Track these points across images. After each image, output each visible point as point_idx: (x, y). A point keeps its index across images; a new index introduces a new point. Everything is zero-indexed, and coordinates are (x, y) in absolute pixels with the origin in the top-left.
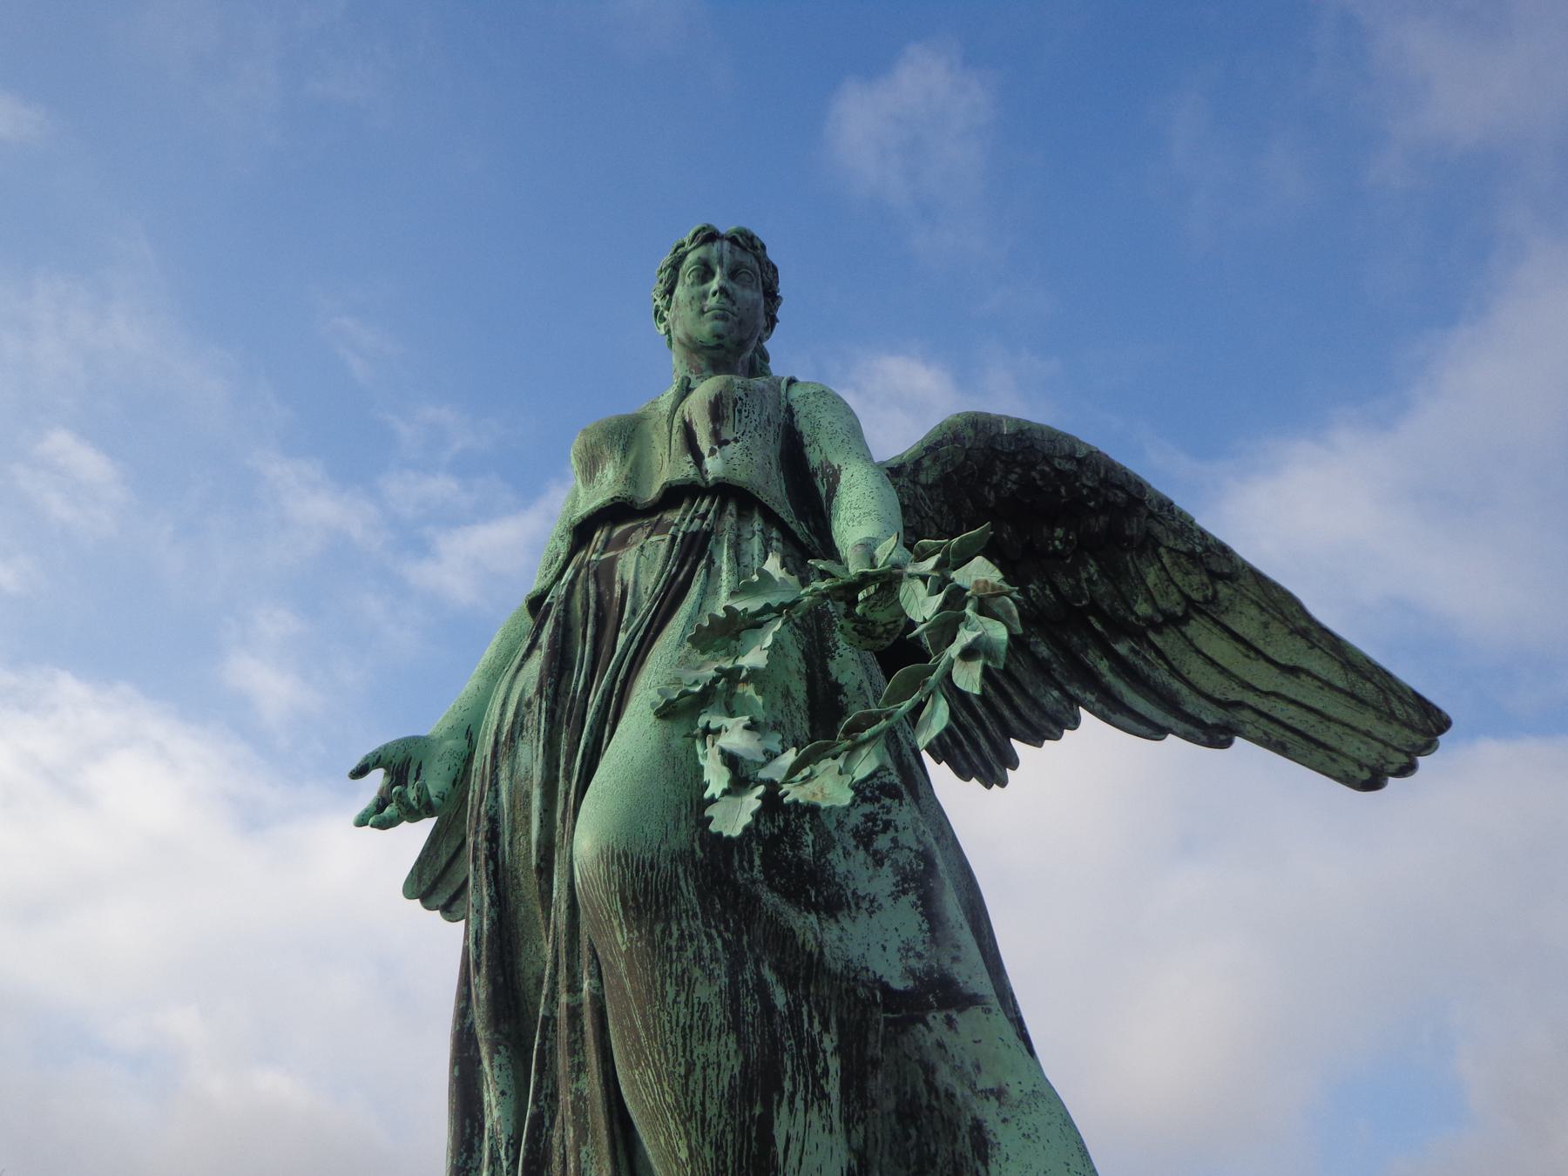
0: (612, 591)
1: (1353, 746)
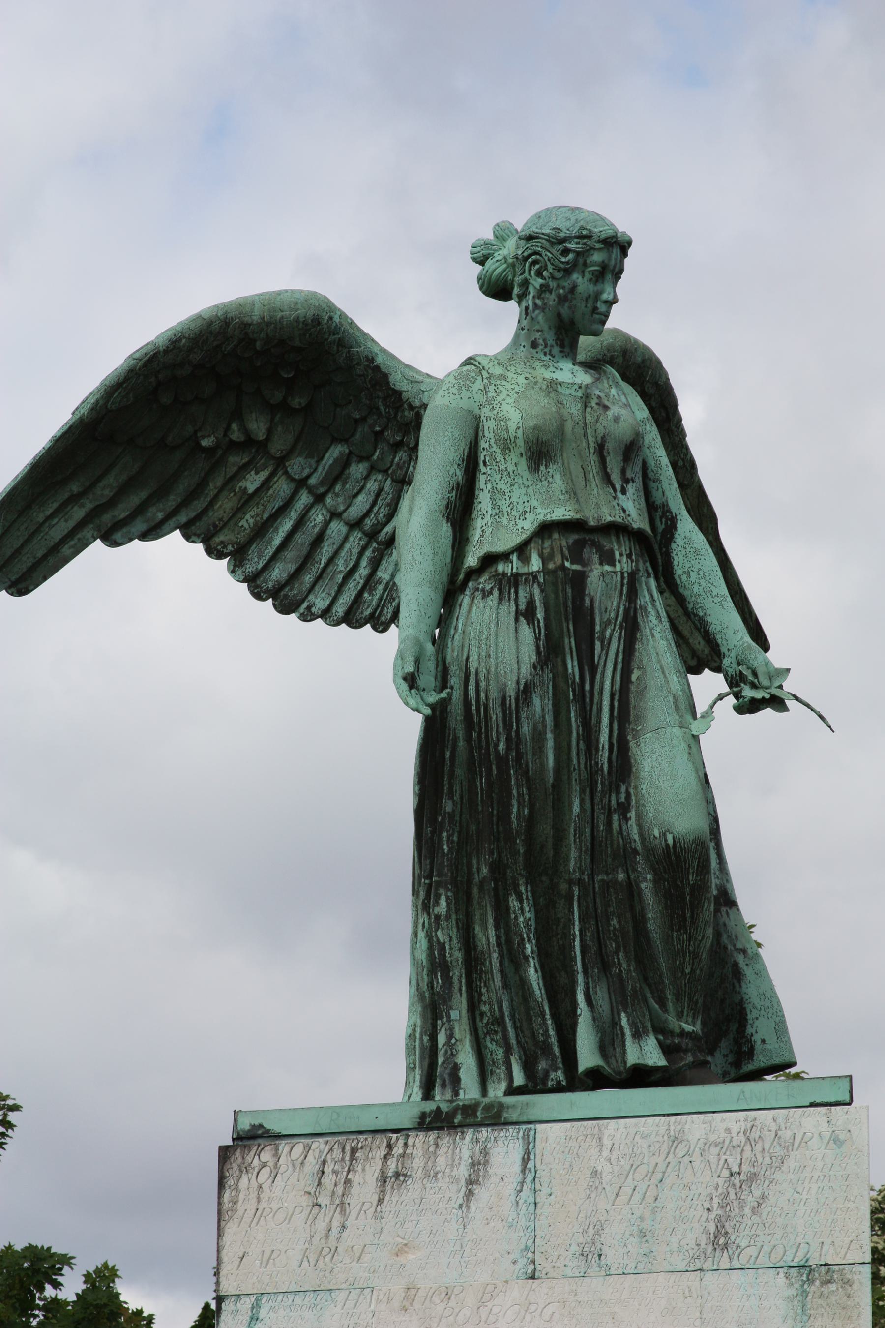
0: (583, 600)
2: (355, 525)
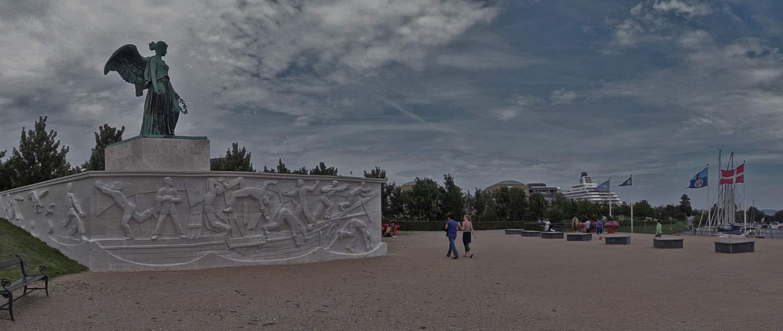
2: (134, 73)
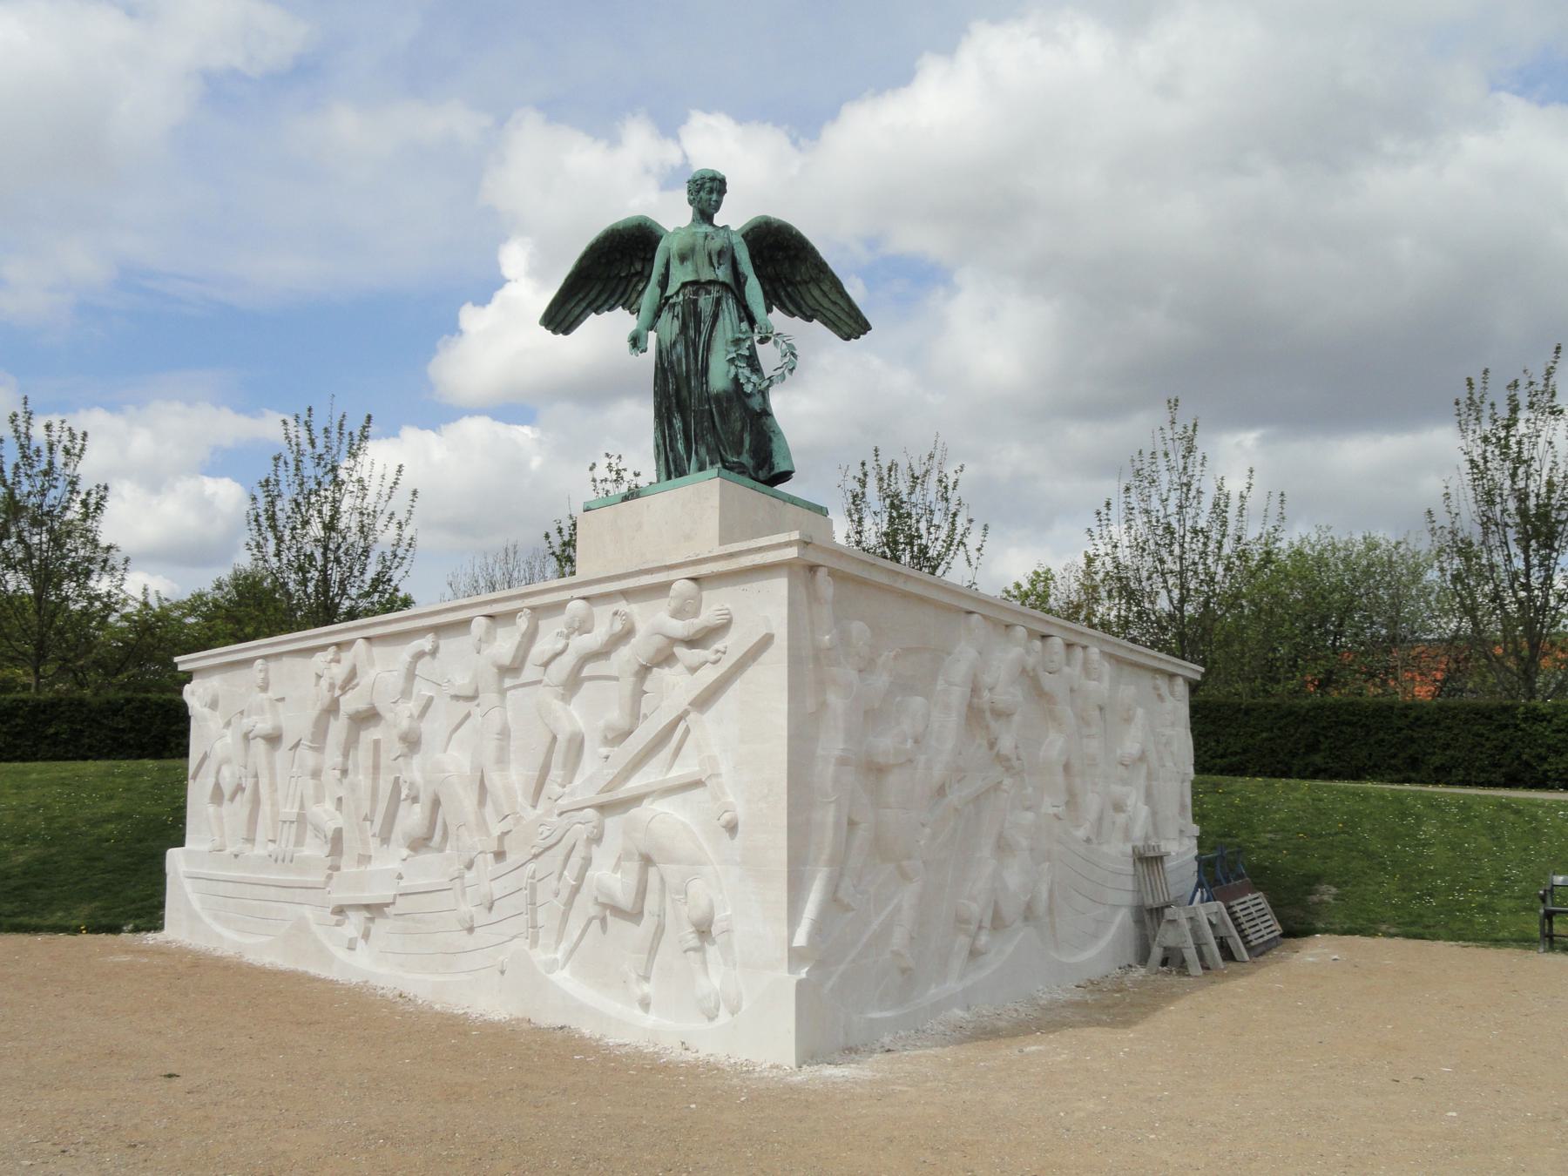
1: (846, 329)
